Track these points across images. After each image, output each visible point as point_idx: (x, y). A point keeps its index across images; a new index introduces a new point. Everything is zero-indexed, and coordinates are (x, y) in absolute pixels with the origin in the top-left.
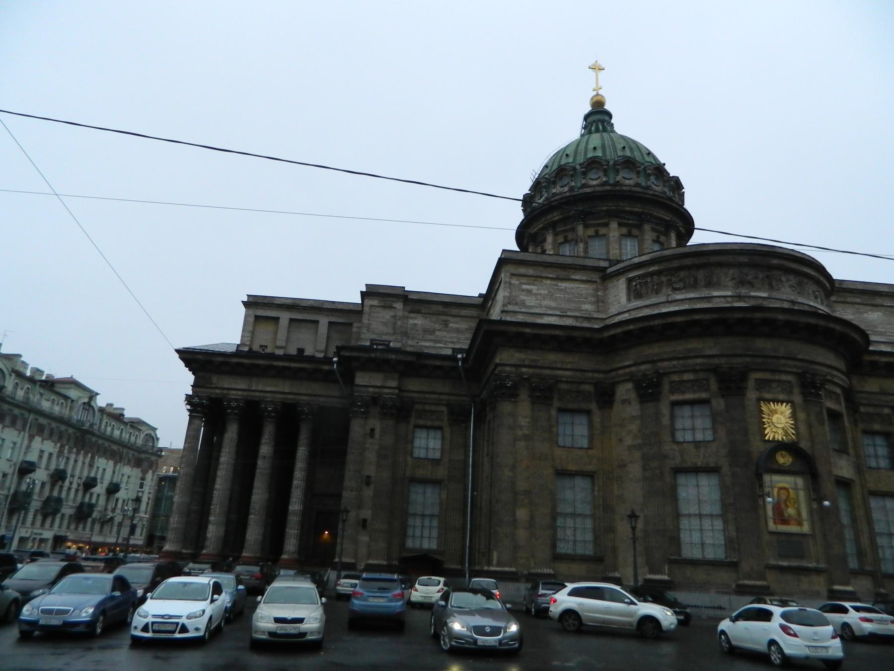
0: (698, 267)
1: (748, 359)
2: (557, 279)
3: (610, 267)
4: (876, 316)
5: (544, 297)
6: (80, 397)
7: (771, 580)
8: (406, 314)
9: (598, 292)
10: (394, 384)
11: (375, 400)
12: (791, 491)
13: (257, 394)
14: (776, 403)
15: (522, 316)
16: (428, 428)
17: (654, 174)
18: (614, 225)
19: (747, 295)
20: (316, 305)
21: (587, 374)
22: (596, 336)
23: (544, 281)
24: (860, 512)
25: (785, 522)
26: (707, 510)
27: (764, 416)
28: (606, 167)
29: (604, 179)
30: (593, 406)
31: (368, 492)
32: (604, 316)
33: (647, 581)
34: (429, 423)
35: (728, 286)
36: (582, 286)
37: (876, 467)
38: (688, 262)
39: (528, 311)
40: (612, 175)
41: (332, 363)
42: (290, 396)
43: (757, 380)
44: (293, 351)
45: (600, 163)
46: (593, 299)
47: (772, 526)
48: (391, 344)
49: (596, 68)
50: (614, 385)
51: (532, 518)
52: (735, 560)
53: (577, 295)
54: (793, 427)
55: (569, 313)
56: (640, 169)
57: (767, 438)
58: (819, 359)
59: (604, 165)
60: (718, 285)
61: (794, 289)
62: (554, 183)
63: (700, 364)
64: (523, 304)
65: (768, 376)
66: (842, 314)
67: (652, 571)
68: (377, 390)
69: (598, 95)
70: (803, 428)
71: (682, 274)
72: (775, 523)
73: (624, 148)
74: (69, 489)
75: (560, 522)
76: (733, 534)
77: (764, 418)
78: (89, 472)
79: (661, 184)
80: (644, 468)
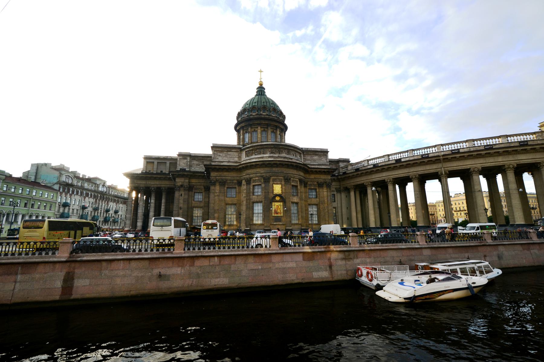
0: (261, 148)
1: (271, 174)
5: (224, 157)
6: (100, 183)
10: (187, 181)
13: (149, 185)
16: (199, 193)
18: (259, 128)
22: (236, 167)
25: (277, 213)
29: (257, 113)
30: (237, 186)
31: (181, 211)
34: (198, 191)
36: (235, 153)
38: (258, 147)
40: (259, 112)
42: (159, 185)
44: (159, 172)
46: (238, 157)
47: (273, 215)
49: (261, 71)
50: (242, 180)
51: (219, 216)
60: (266, 153)
62: (243, 114)
68: (182, 183)
69: (261, 81)
70: (283, 191)
71: (258, 150)
74: (101, 213)
75: (227, 216)
78: (107, 207)
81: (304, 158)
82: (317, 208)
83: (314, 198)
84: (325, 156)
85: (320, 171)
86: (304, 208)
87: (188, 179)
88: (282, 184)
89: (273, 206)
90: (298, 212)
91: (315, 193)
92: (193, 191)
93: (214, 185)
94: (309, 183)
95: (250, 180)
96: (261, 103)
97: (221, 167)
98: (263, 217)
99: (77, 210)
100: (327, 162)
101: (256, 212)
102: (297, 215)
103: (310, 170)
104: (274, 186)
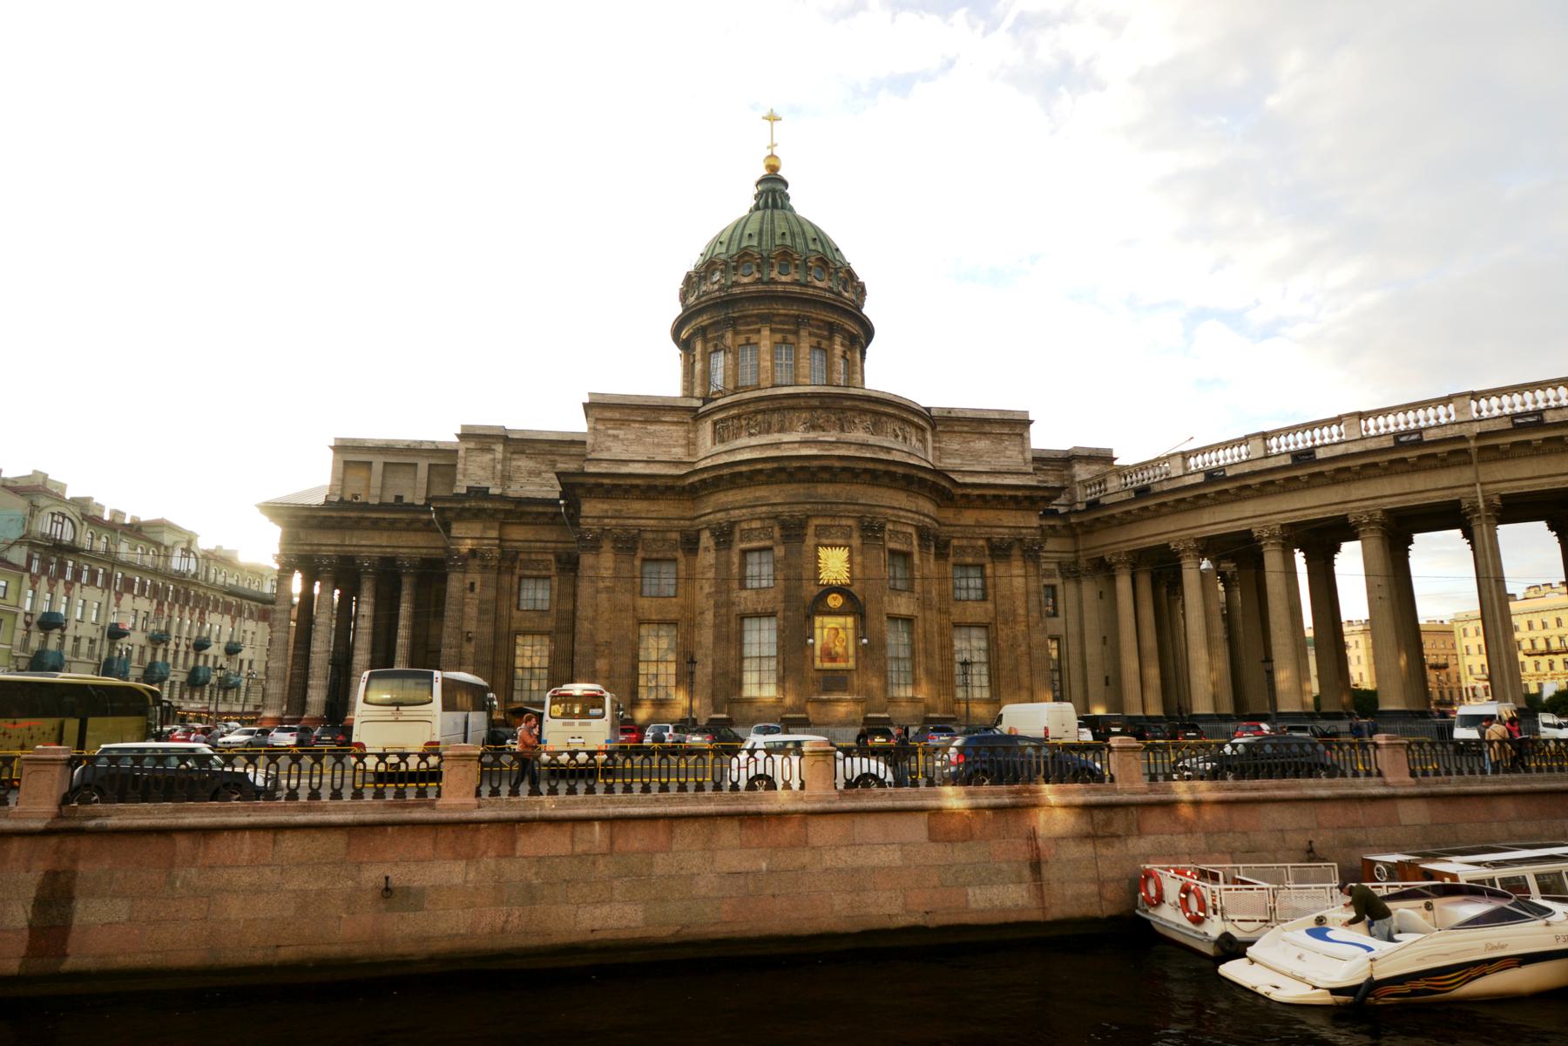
0: (773, 410)
1: (808, 506)
2: (646, 422)
3: (704, 405)
5: (632, 442)
6: (175, 543)
8: (509, 455)
10: (494, 534)
12: (840, 631)
13: (352, 549)
16: (536, 578)
18: (766, 332)
21: (672, 522)
22: (680, 483)
25: (833, 659)
26: (765, 652)
28: (759, 261)
29: (757, 275)
30: (679, 555)
32: (695, 460)
33: (711, 720)
34: (535, 573)
38: (763, 406)
40: (766, 272)
41: (431, 513)
42: (388, 550)
43: (816, 526)
44: (390, 499)
46: (684, 442)
47: (818, 664)
48: (491, 491)
50: (698, 532)
51: (611, 669)
60: (791, 429)
62: (705, 278)
65: (828, 522)
67: (716, 712)
69: (772, 156)
70: (857, 571)
71: (759, 417)
72: (821, 661)
73: (784, 234)
74: (176, 652)
75: (642, 668)
76: (781, 672)
78: (200, 630)
80: (715, 616)
81: (934, 448)
82: (988, 639)
83: (976, 600)
84: (1018, 440)
86: (937, 638)
87: (497, 525)
88: (850, 546)
89: (818, 632)
90: (913, 653)
91: (979, 582)
92: (517, 571)
94: (955, 542)
95: (731, 533)
96: (773, 238)
97: (622, 482)
98: (777, 670)
99: (92, 641)
100: (1026, 463)
101: (754, 654)
102: (908, 665)
103: (960, 491)
104: (823, 552)
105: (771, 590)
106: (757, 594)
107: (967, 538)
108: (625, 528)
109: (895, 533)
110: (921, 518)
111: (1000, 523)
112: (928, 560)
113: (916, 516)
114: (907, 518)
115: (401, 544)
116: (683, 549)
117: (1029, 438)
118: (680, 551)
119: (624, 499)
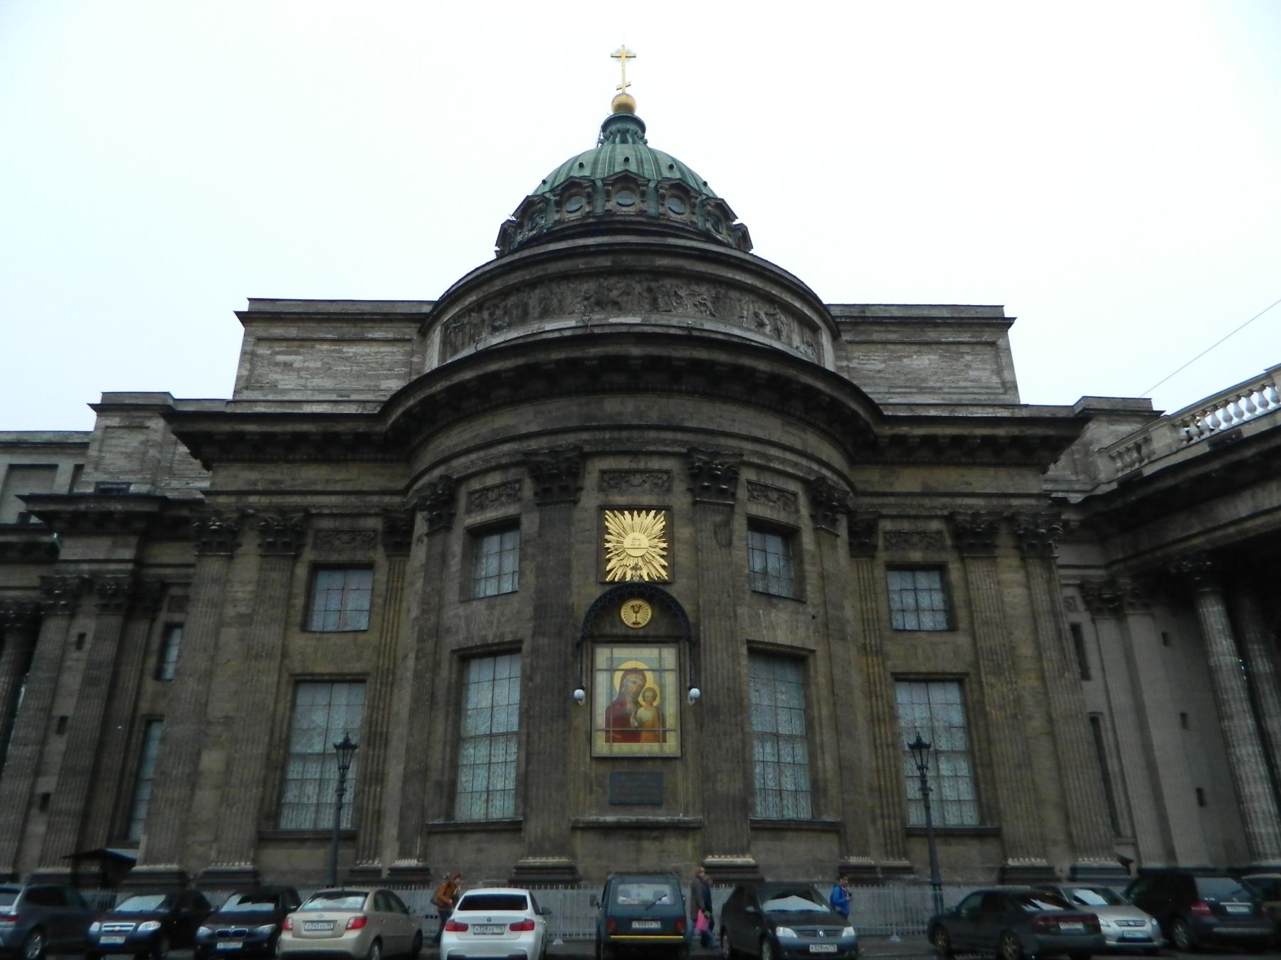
0: (532, 284)
1: (585, 436)
4: (927, 362)
5: (314, 373)
7: (586, 852)
9: (412, 357)
11: (88, 585)
12: (649, 675)
14: (635, 513)
15: (265, 407)
17: (673, 196)
19: (604, 322)
20: (56, 439)
21: (368, 498)
23: (318, 346)
24: (823, 711)
25: (633, 736)
27: (607, 537)
29: (587, 209)
30: (379, 556)
31: (58, 745)
35: (573, 312)
36: (386, 349)
37: (916, 628)
39: (279, 398)
43: (603, 472)
45: (579, 185)
52: (521, 819)
53: (373, 365)
54: (665, 553)
55: (354, 397)
56: (644, 188)
57: (609, 578)
58: (727, 427)
59: (586, 187)
60: (561, 312)
61: (703, 308)
63: (508, 454)
64: (273, 387)
65: (625, 463)
66: (862, 362)
68: (95, 567)
69: (623, 93)
70: (683, 556)
71: (512, 300)
72: (607, 740)
75: (294, 770)
76: (523, 764)
77: (609, 542)
79: (688, 211)
82: (965, 704)
84: (988, 354)
85: (957, 441)
87: (134, 540)
89: (601, 679)
90: (809, 725)
91: (938, 599)
93: (221, 546)
94: (886, 525)
97: (277, 428)
98: (518, 761)
102: (801, 753)
103: (887, 431)
104: (613, 522)
105: (516, 598)
106: (491, 607)
107: (909, 517)
108: (282, 511)
109: (760, 491)
110: (815, 467)
111: (968, 490)
112: (834, 547)
113: (804, 462)
114: (784, 461)
115: (11, 583)
116: (386, 546)
117: (1008, 349)
118: (381, 549)
119: (287, 461)
